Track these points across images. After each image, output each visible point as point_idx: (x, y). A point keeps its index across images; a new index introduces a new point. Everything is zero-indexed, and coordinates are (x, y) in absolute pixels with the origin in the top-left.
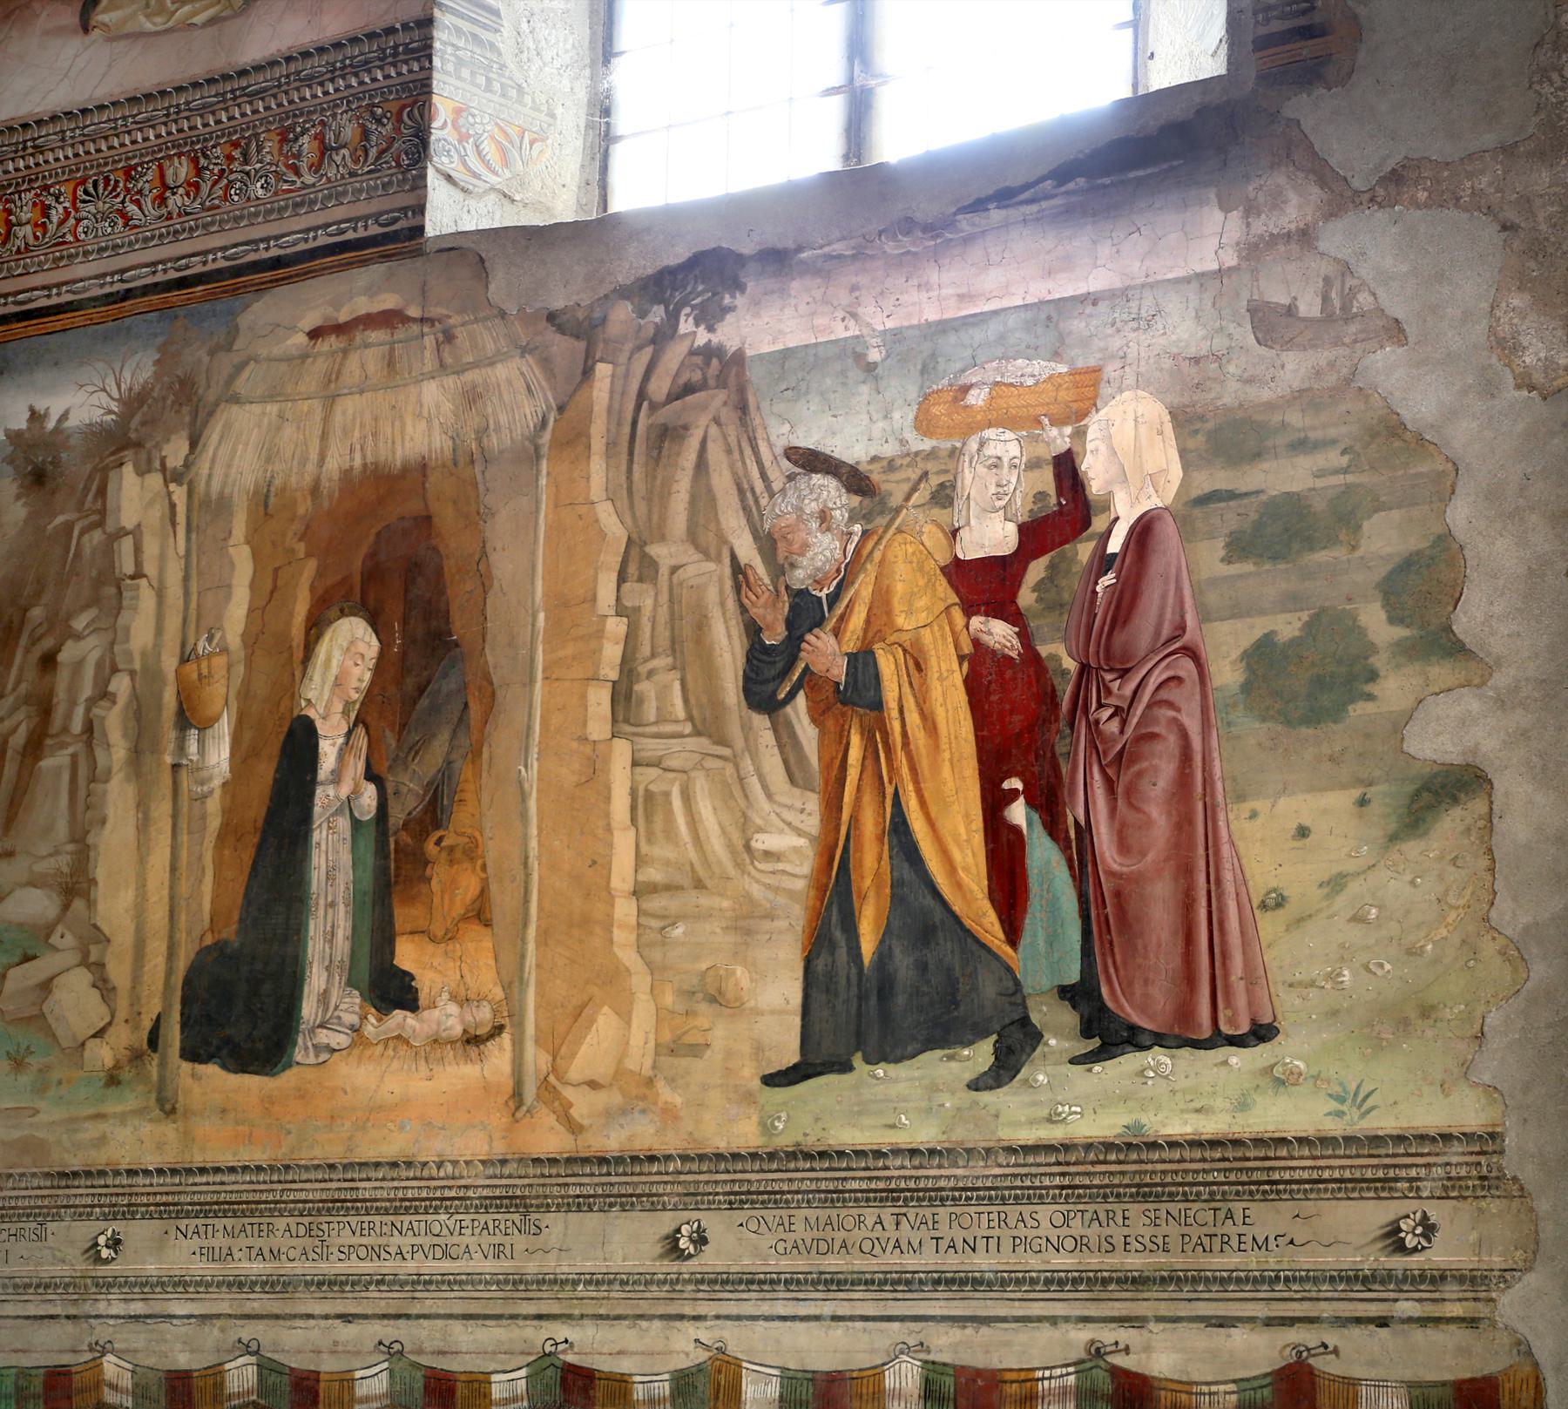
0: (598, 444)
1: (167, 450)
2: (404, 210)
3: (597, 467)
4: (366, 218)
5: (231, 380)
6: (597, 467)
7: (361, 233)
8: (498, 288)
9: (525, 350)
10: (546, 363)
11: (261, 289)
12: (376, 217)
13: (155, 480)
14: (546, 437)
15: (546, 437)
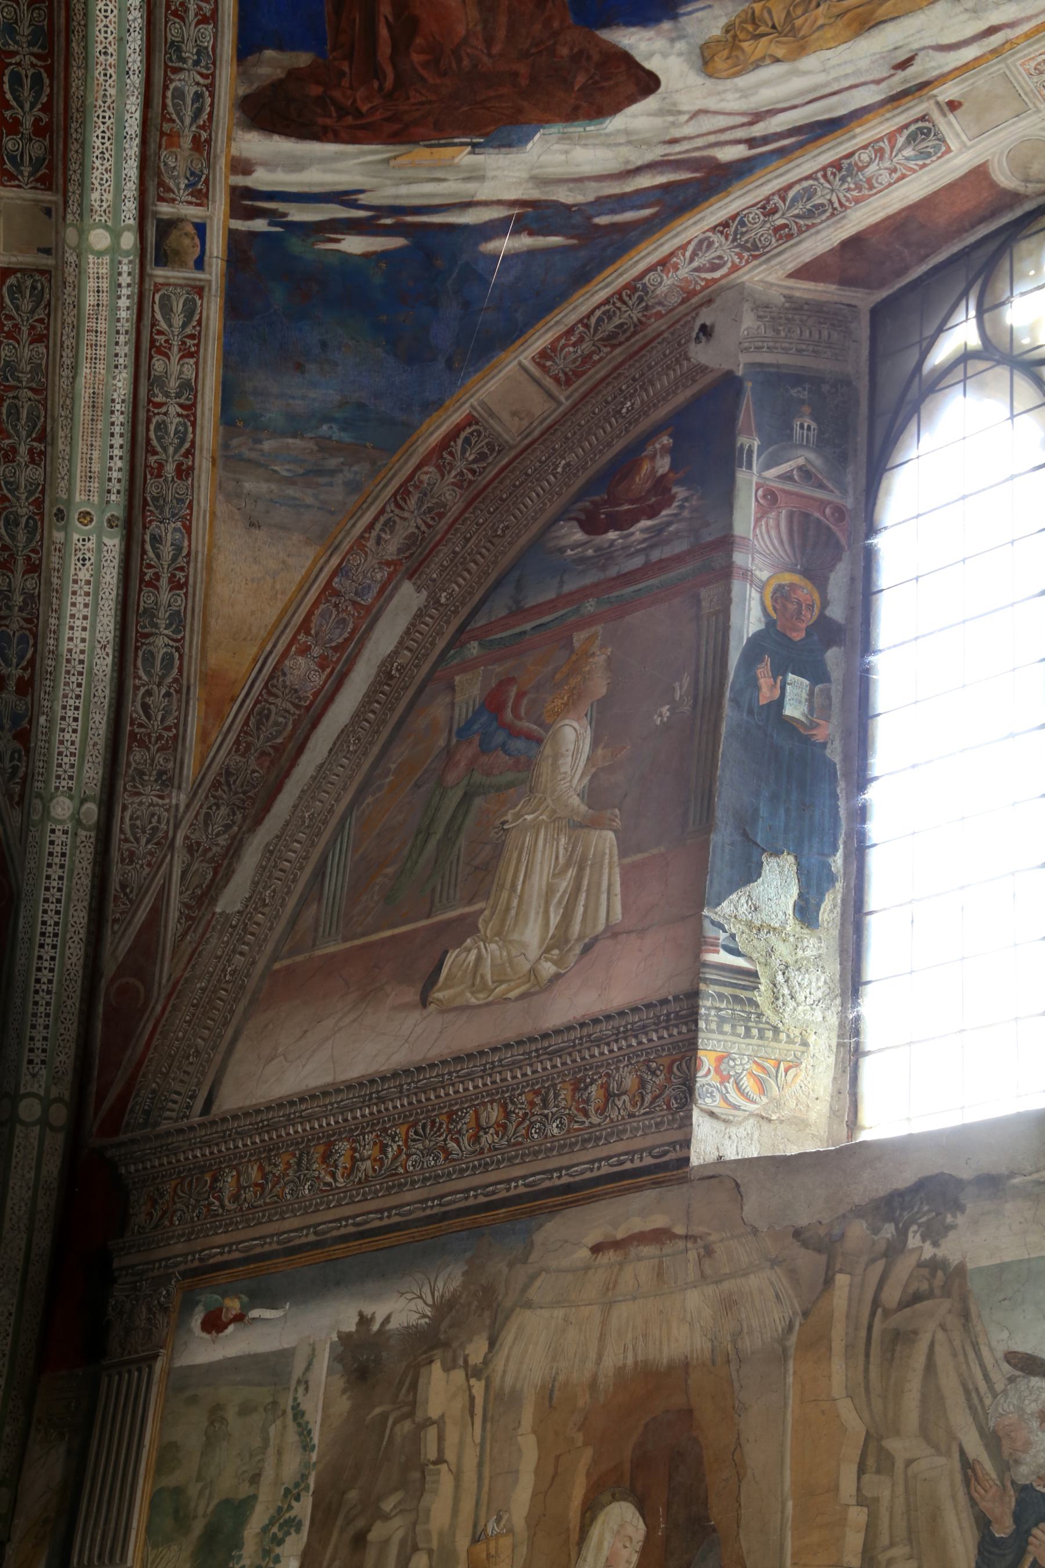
0: (838, 1345)
1: (470, 1349)
2: (673, 1144)
3: (837, 1366)
4: (641, 1151)
5: (525, 1288)
6: (837, 1366)
7: (637, 1164)
8: (751, 1208)
9: (774, 1263)
10: (793, 1274)
11: (553, 1211)
12: (650, 1150)
13: (458, 1375)
14: (793, 1339)
15: (793, 1339)
